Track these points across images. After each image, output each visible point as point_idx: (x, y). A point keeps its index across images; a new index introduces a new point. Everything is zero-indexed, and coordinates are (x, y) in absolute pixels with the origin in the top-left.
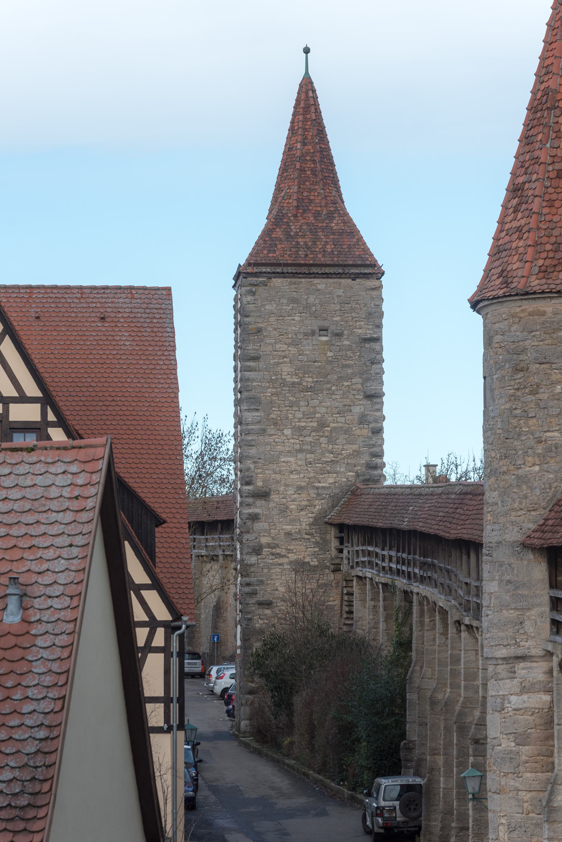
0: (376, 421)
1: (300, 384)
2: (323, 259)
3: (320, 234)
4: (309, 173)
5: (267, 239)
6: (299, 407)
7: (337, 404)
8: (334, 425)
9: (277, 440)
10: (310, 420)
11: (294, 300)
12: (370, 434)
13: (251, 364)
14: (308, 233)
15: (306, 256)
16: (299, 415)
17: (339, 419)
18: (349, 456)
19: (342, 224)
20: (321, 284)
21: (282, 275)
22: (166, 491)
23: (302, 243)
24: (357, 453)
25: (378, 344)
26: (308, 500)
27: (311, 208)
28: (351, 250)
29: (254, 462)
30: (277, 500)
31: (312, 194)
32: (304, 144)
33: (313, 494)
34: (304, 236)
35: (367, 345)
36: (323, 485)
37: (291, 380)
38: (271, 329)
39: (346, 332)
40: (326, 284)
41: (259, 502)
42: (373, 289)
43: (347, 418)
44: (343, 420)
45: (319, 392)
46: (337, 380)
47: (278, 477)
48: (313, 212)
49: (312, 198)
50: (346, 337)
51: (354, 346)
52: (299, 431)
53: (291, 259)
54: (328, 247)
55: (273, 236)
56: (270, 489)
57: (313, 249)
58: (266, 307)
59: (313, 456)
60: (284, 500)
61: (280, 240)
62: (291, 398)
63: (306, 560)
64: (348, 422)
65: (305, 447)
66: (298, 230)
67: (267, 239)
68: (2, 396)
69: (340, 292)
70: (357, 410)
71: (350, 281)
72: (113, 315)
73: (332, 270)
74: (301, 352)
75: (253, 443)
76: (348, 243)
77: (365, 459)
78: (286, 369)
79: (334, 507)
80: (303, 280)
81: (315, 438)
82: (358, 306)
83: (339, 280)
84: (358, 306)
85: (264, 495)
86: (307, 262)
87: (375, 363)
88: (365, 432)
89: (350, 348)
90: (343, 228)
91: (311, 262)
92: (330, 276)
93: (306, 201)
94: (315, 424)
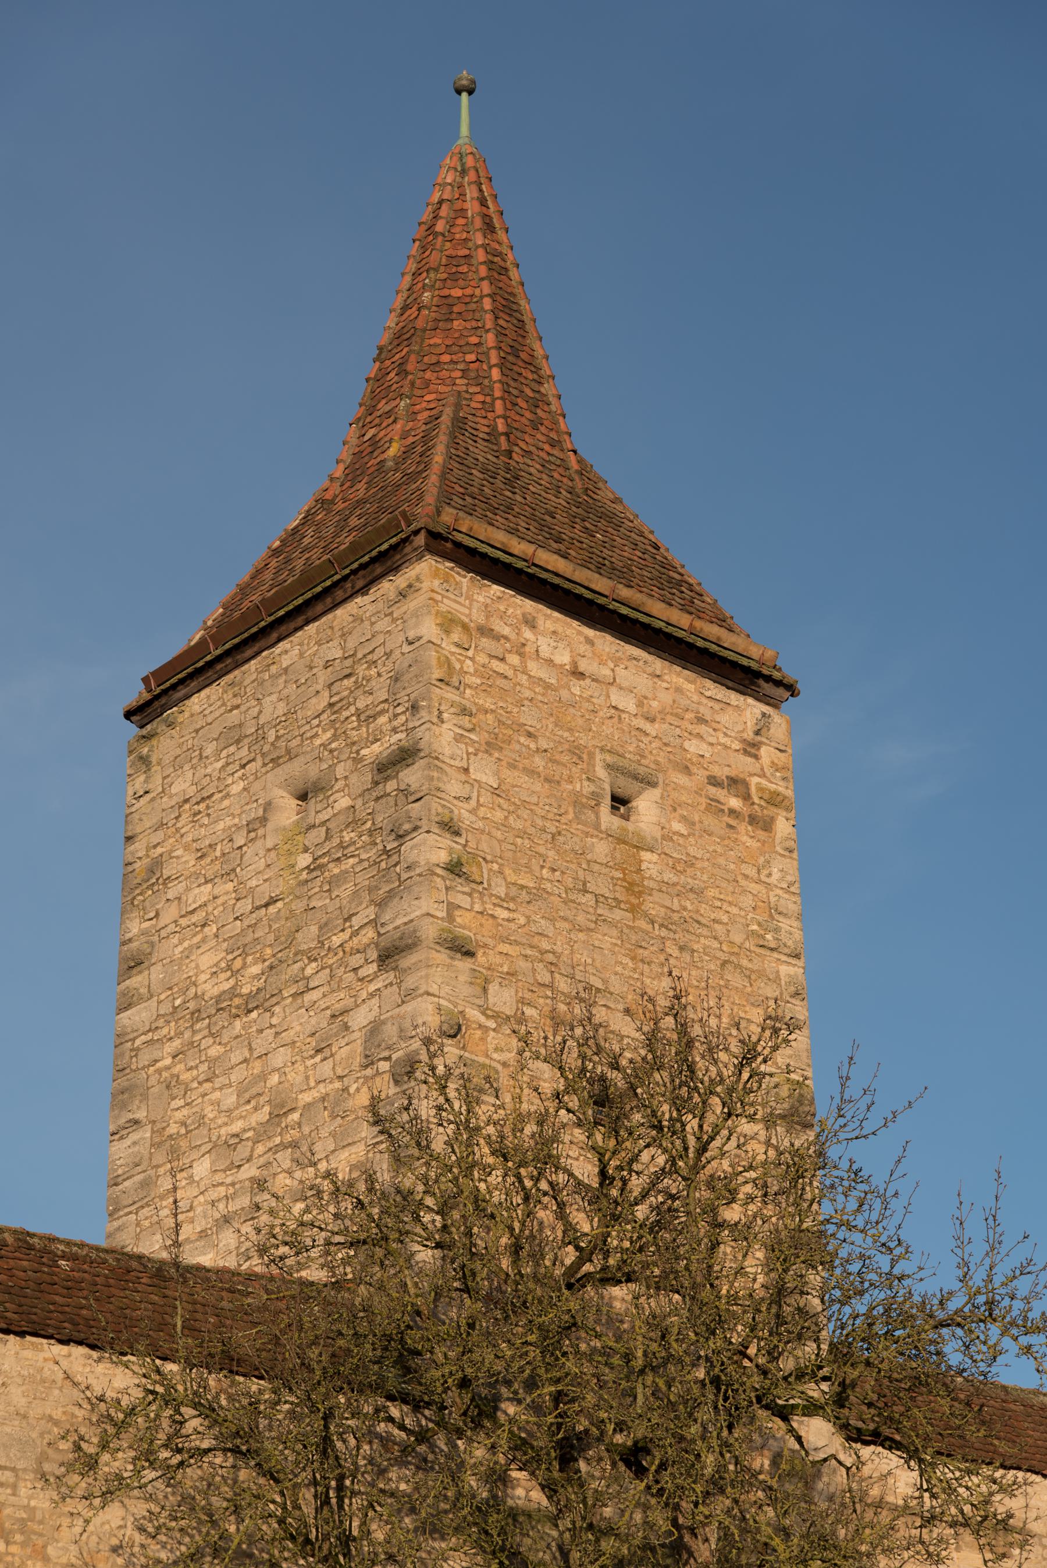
1: (233, 993)
8: (306, 1098)
10: (253, 1103)
25: (420, 764)
35: (391, 786)
37: (216, 991)
40: (301, 644)
42: (402, 595)
45: (274, 1000)
58: (174, 790)
64: (339, 1072)
69: (334, 652)
81: (262, 1161)
83: (330, 616)
87: (407, 833)
92: (310, 614)
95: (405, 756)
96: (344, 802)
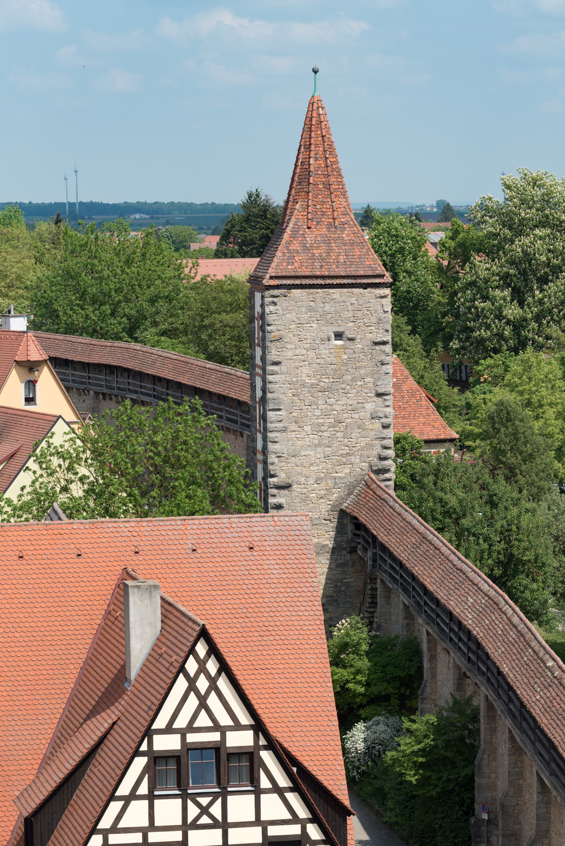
0: (386, 417)
2: (336, 270)
3: (333, 245)
4: (321, 186)
5: (285, 251)
6: (317, 405)
7: (351, 403)
9: (297, 436)
11: (311, 309)
12: (381, 428)
13: (275, 368)
14: (322, 245)
15: (322, 267)
16: (318, 412)
17: (353, 415)
18: (362, 449)
19: (352, 235)
20: (336, 293)
21: (302, 287)
22: (320, 719)
23: (317, 255)
24: (369, 446)
26: (326, 490)
27: (323, 220)
28: (361, 260)
29: (278, 457)
30: (299, 490)
31: (325, 206)
32: (316, 159)
33: (330, 483)
34: (318, 248)
35: (378, 348)
36: (339, 475)
37: (310, 381)
38: (291, 336)
39: (358, 337)
41: (282, 492)
42: (382, 297)
43: (361, 414)
44: (356, 416)
46: (352, 380)
47: (299, 469)
48: (326, 223)
49: (325, 210)
50: (359, 340)
51: (366, 348)
52: (318, 429)
53: (309, 270)
54: (341, 257)
55: (291, 248)
56: (293, 481)
57: (328, 260)
58: (287, 316)
59: (330, 449)
60: (305, 490)
61: (297, 252)
62: (310, 398)
63: (326, 543)
65: (324, 441)
66: (313, 242)
67: (285, 251)
68: (220, 726)
69: (353, 300)
70: (370, 406)
71: (361, 290)
72: (260, 544)
73: (346, 281)
74: (319, 356)
75: (276, 440)
76: (359, 253)
77: (377, 450)
78: (305, 370)
79: (349, 494)
80: (319, 290)
82: (368, 313)
84: (368, 313)
85: (287, 487)
86: (323, 273)
88: (377, 425)
89: (363, 351)
90: (353, 238)
91: (326, 273)
93: (319, 213)
94: (332, 421)
95: (384, 343)
96: (361, 346)
